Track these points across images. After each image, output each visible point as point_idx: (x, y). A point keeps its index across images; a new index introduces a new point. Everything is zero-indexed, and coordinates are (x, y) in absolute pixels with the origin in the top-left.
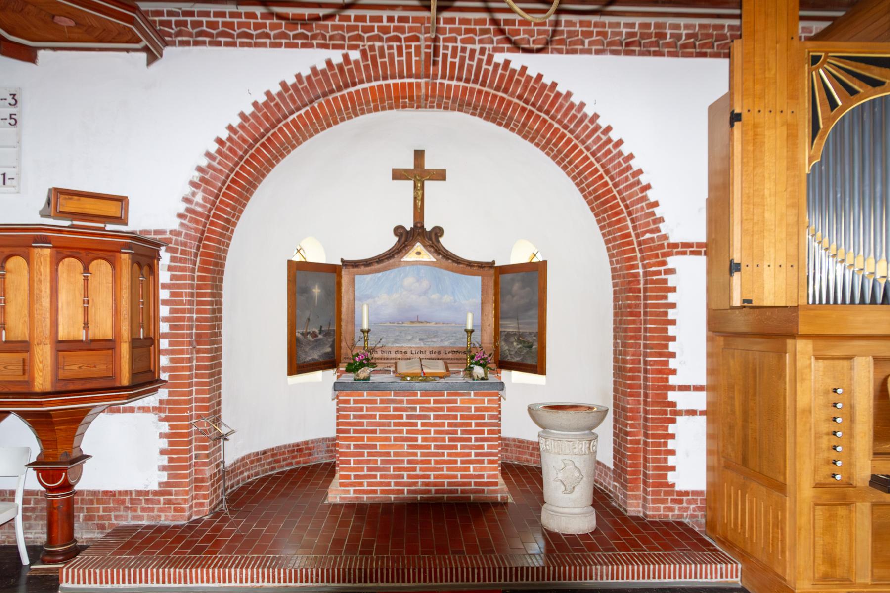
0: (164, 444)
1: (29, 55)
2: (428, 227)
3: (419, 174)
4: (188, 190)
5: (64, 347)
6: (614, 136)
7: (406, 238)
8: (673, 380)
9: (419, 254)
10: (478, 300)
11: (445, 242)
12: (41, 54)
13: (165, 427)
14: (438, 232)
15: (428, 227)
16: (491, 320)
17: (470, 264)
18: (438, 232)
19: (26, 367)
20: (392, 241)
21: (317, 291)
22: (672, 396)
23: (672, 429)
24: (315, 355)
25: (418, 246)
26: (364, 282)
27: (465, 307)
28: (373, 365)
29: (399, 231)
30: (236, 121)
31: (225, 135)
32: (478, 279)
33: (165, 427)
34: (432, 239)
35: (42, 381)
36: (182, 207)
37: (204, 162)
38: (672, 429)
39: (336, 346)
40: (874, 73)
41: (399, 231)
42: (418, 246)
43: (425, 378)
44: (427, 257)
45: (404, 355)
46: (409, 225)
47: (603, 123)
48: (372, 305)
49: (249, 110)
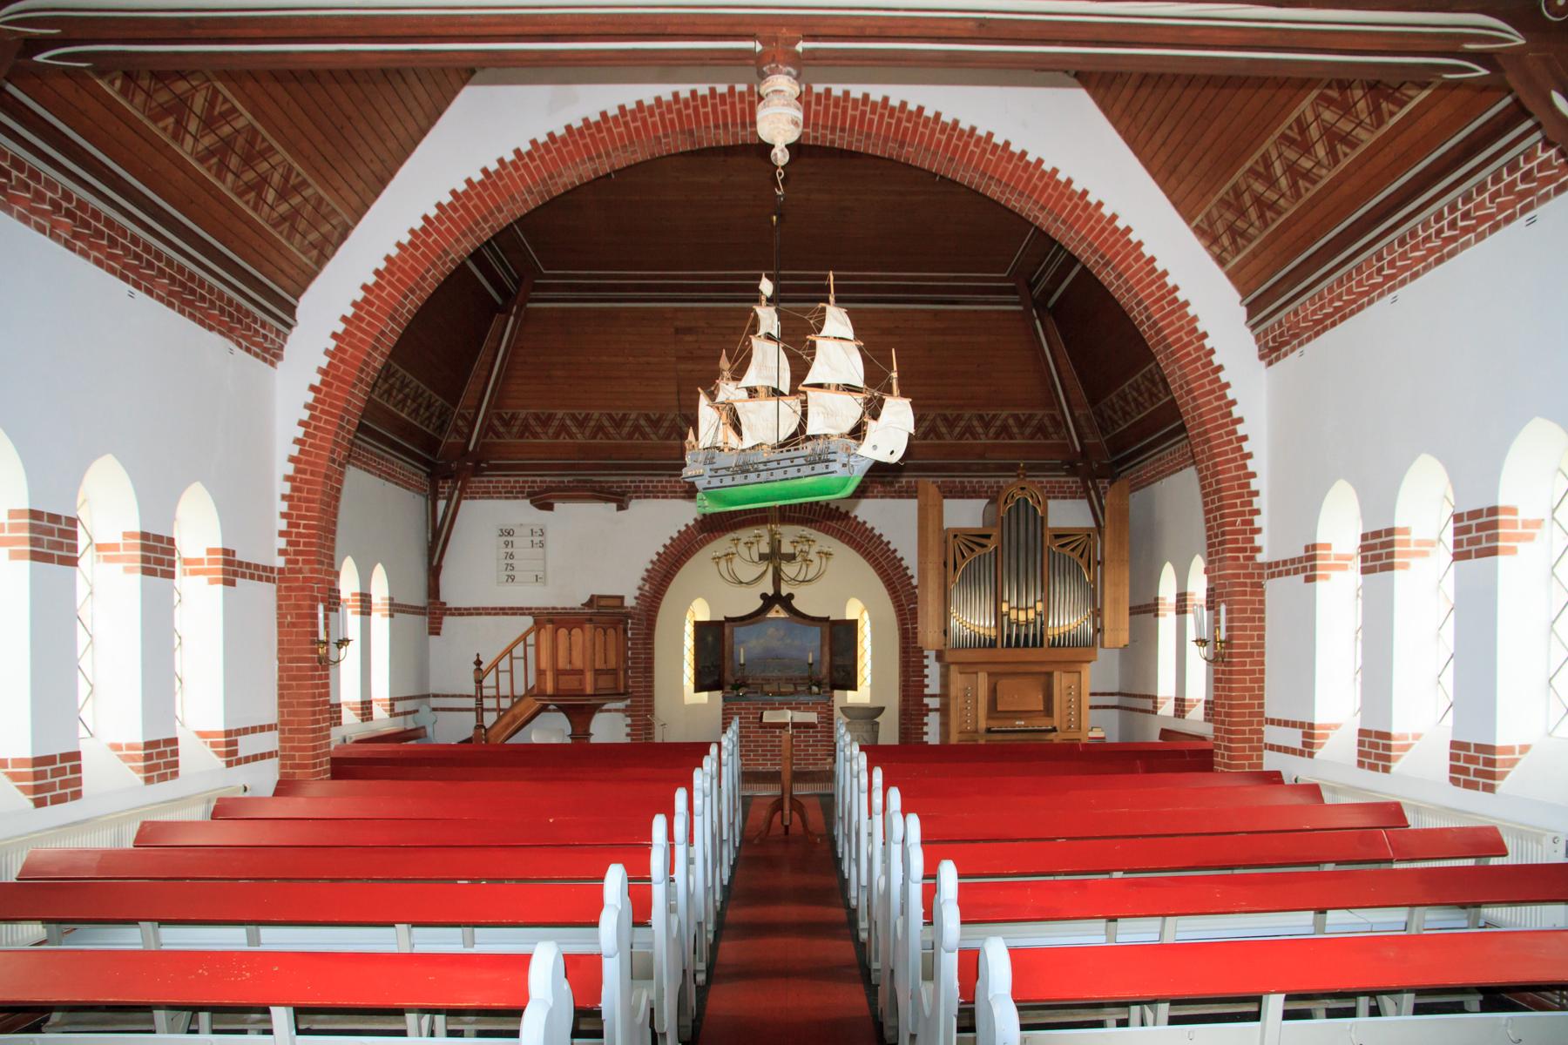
0: (628, 730)
1: (550, 507)
2: (784, 593)
3: (775, 557)
4: (641, 583)
5: (598, 672)
6: (892, 547)
7: (769, 601)
8: (927, 691)
9: (777, 613)
10: (817, 643)
11: (795, 603)
12: (556, 505)
13: (629, 721)
14: (791, 596)
15: (784, 593)
16: (827, 658)
17: (813, 619)
18: (791, 596)
19: (581, 682)
20: (761, 602)
21: (710, 639)
22: (926, 700)
23: (926, 720)
24: (708, 681)
25: (777, 607)
26: (740, 632)
27: (811, 648)
28: (747, 685)
29: (764, 596)
30: (668, 542)
31: (661, 550)
32: (818, 629)
33: (629, 721)
34: (786, 602)
35: (589, 690)
36: (637, 593)
37: (650, 566)
38: (926, 720)
39: (721, 675)
40: (984, 541)
41: (764, 596)
42: (777, 607)
43: (780, 694)
44: (783, 614)
45: (768, 681)
46: (770, 592)
47: (885, 539)
48: (745, 648)
49: (675, 535)
